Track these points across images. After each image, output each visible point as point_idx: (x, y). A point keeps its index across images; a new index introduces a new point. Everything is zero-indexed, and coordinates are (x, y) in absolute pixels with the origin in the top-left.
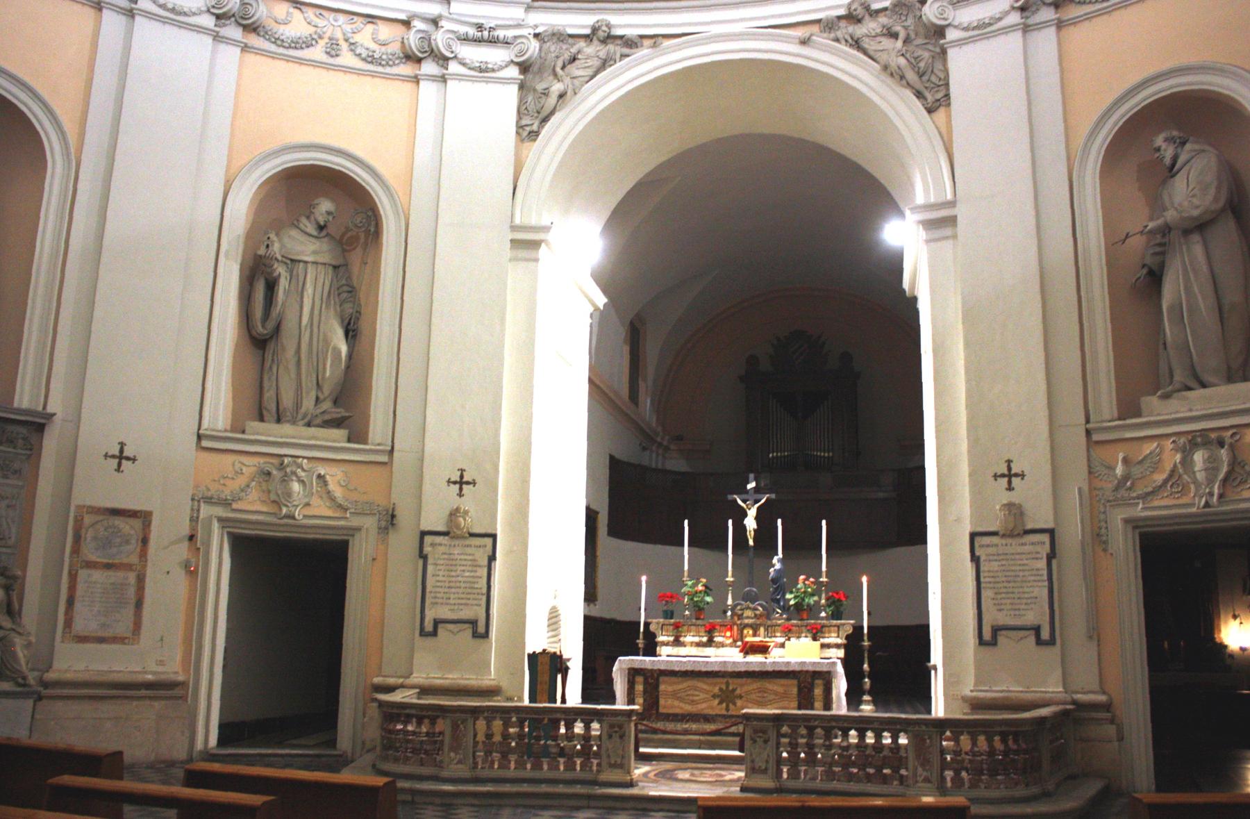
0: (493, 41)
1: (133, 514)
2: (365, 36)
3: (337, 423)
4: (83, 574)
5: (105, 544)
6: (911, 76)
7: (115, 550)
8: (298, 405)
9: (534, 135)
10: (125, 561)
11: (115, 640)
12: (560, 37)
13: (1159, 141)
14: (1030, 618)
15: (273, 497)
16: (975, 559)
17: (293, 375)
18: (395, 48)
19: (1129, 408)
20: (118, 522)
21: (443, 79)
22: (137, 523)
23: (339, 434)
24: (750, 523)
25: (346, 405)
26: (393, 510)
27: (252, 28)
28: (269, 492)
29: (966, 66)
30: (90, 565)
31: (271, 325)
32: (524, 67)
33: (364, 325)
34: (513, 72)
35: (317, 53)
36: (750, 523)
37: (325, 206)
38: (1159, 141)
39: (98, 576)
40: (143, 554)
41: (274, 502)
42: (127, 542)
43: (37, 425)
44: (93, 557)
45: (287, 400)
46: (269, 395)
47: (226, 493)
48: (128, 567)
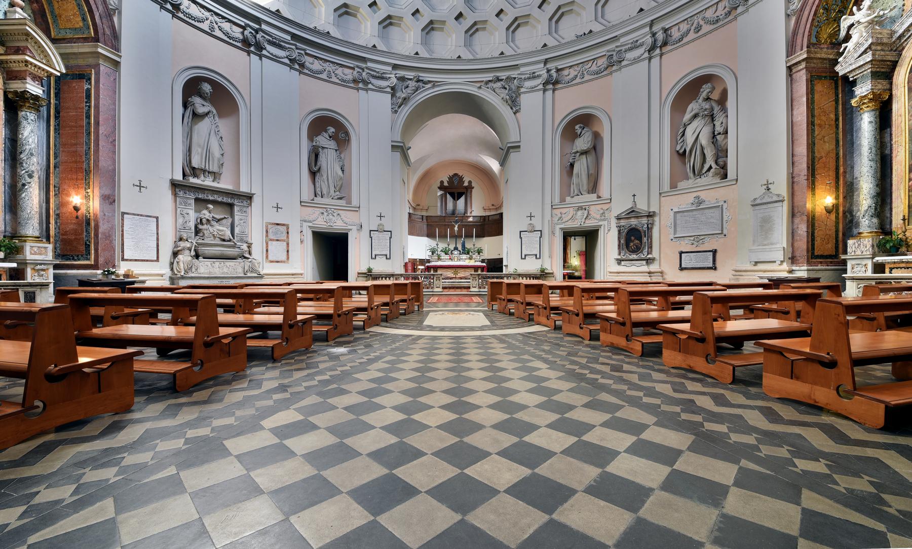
0: (382, 78)
1: (284, 225)
2: (340, 71)
3: (340, 198)
4: (270, 243)
6: (509, 102)
8: (329, 192)
9: (396, 112)
11: (281, 262)
12: (402, 79)
13: (577, 127)
14: (534, 253)
16: (521, 238)
18: (350, 77)
19: (563, 200)
20: (279, 227)
21: (367, 90)
24: (456, 228)
25: (343, 191)
27: (302, 65)
29: (526, 100)
30: (271, 240)
32: (393, 88)
33: (345, 168)
34: (389, 90)
35: (324, 76)
36: (456, 228)
37: (331, 130)
38: (577, 127)
39: (274, 243)
40: (288, 237)
43: (249, 197)
44: (272, 238)
45: (325, 192)
46: (318, 190)
48: (283, 241)
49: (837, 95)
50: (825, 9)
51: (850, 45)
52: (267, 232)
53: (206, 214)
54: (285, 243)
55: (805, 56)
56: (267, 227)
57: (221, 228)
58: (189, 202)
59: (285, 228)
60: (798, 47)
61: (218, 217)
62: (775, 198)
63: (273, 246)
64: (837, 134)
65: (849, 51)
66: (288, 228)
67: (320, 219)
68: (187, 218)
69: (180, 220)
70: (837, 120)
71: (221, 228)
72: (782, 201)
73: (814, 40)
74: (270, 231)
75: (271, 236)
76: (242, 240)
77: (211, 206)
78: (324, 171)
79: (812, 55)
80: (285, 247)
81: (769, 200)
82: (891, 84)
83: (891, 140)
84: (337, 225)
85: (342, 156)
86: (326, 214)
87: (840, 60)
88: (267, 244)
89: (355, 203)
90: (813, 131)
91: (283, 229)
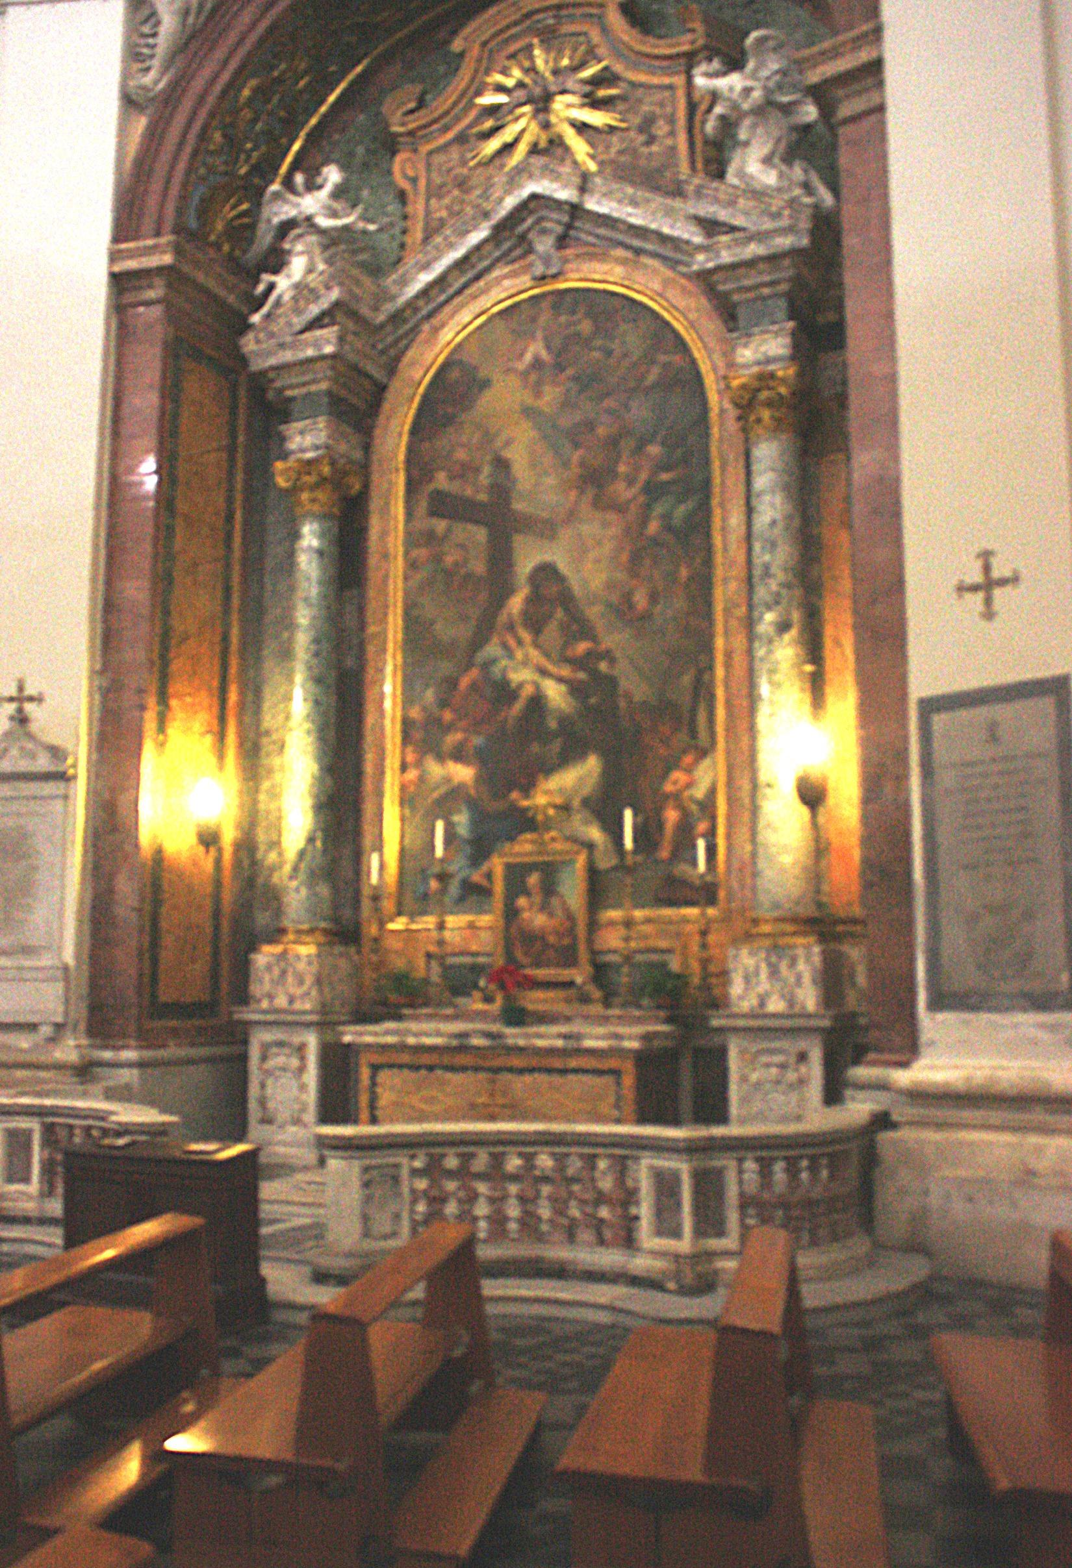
49: (233, 435)
50: (225, 136)
51: (283, 283)
55: (168, 259)
60: (148, 223)
62: (43, 763)
64: (228, 566)
65: (278, 303)
70: (230, 518)
72: (63, 777)
73: (193, 223)
79: (186, 269)
81: (24, 766)
82: (367, 447)
83: (362, 627)
87: (256, 318)
90: (170, 529)
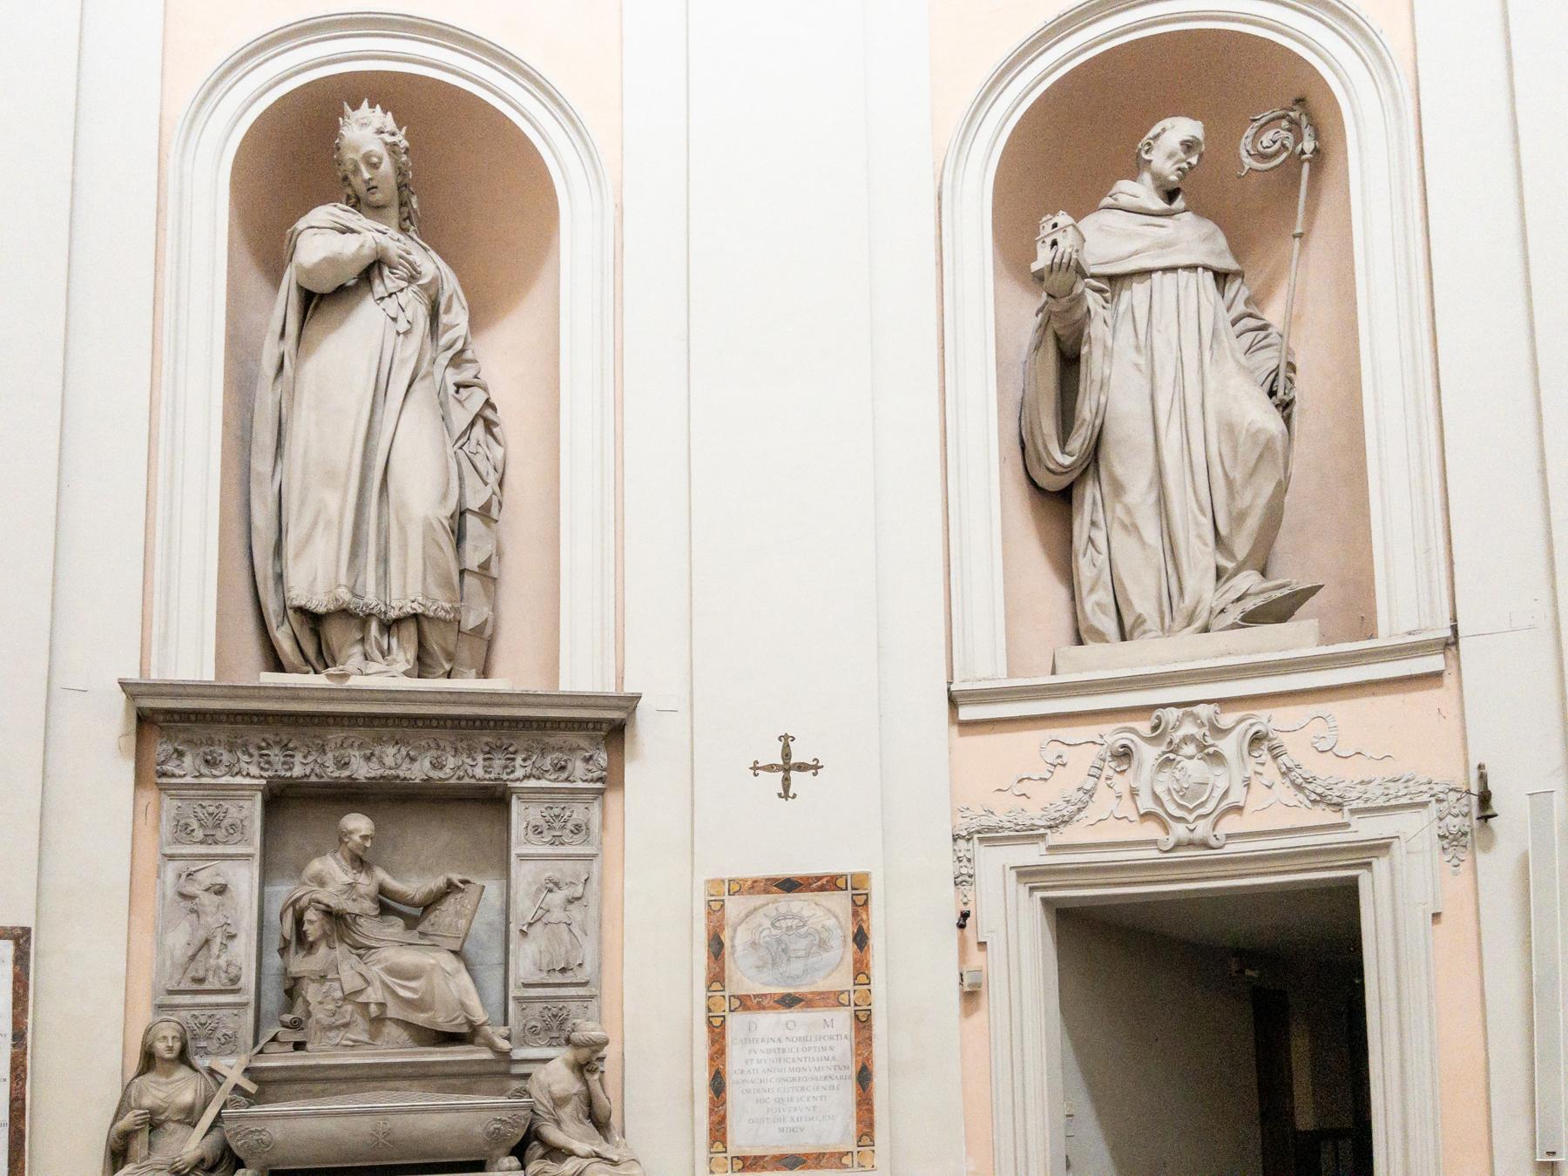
1: (830, 883)
3: (1278, 611)
5: (778, 953)
7: (796, 967)
10: (822, 986)
15: (1146, 803)
17: (1151, 532)
20: (798, 903)
22: (839, 902)
23: (1295, 638)
25: (1286, 565)
26: (1483, 778)
28: (1134, 793)
31: (1078, 442)
41: (1147, 816)
42: (823, 945)
47: (1034, 813)
52: (716, 947)
53: (331, 877)
54: (842, 1019)
56: (715, 911)
57: (409, 958)
58: (233, 811)
59: (839, 902)
61: (414, 886)
63: (759, 1042)
66: (860, 905)
67: (1104, 801)
68: (211, 920)
69: (180, 939)
71: (409, 958)
74: (738, 940)
75: (745, 976)
76: (556, 1028)
77: (358, 824)
78: (1129, 464)
80: (843, 1048)
84: (1250, 822)
85: (1274, 313)
86: (1149, 755)
88: (717, 1034)
89: (1403, 610)
91: (826, 914)
